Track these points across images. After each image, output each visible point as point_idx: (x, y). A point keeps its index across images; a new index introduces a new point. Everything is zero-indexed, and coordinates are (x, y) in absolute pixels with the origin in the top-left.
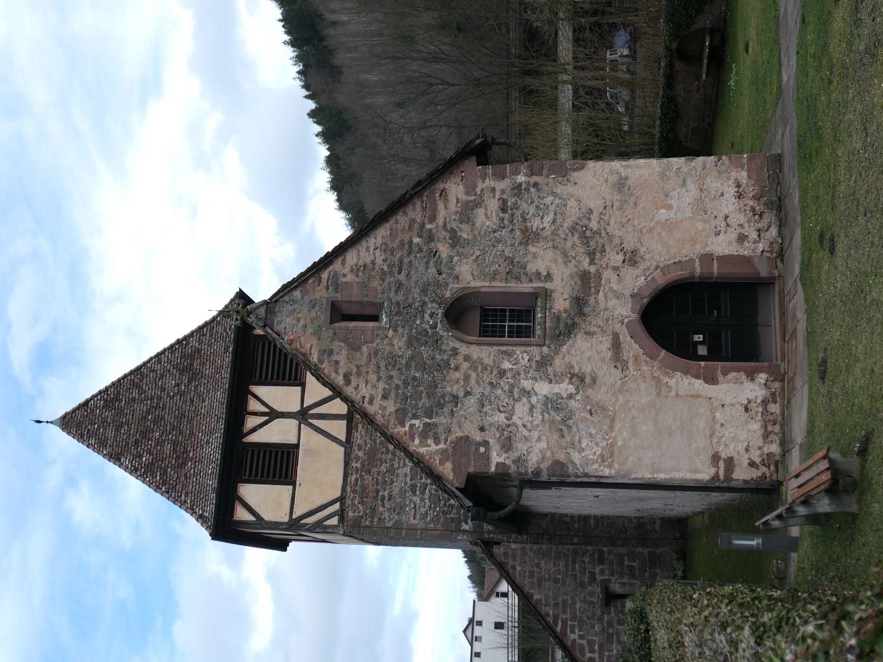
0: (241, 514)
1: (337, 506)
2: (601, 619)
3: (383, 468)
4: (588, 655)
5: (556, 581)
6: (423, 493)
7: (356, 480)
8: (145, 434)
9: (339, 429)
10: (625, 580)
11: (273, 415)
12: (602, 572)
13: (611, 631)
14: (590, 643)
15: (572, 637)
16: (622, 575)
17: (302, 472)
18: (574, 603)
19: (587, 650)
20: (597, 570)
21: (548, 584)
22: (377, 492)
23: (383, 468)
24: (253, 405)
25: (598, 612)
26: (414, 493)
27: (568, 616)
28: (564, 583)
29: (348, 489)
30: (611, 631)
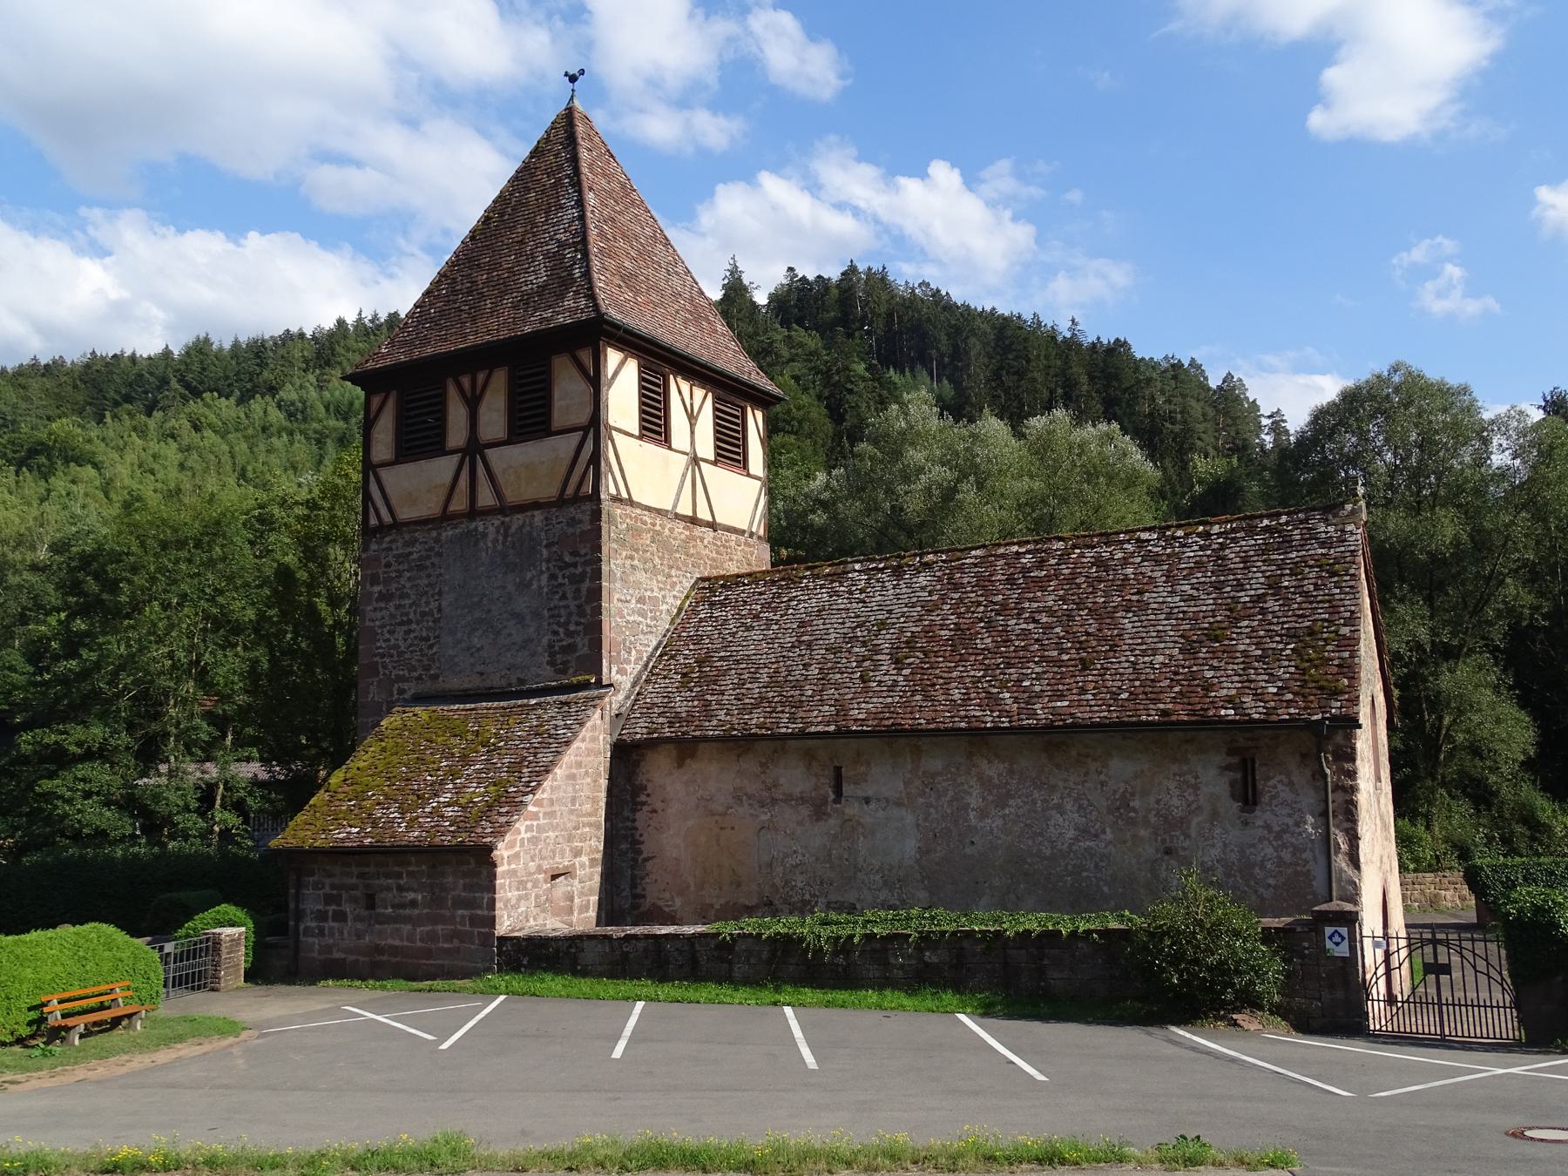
0: (613, 357)
1: (625, 495)
2: (539, 869)
3: (657, 561)
4: (506, 854)
5: (574, 800)
6: (640, 614)
7: (645, 523)
8: (624, 236)
9: (685, 509)
10: (576, 900)
11: (692, 418)
12: (582, 866)
13: (529, 885)
14: (517, 855)
15: (523, 829)
16: (582, 894)
17: (651, 449)
18: (554, 828)
19: (511, 852)
20: (584, 859)
21: (570, 789)
22: (637, 550)
23: (657, 561)
24: (699, 393)
25: (546, 865)
26: (638, 601)
27: (542, 821)
28: (571, 812)
29: (638, 511)
30: (529, 885)
